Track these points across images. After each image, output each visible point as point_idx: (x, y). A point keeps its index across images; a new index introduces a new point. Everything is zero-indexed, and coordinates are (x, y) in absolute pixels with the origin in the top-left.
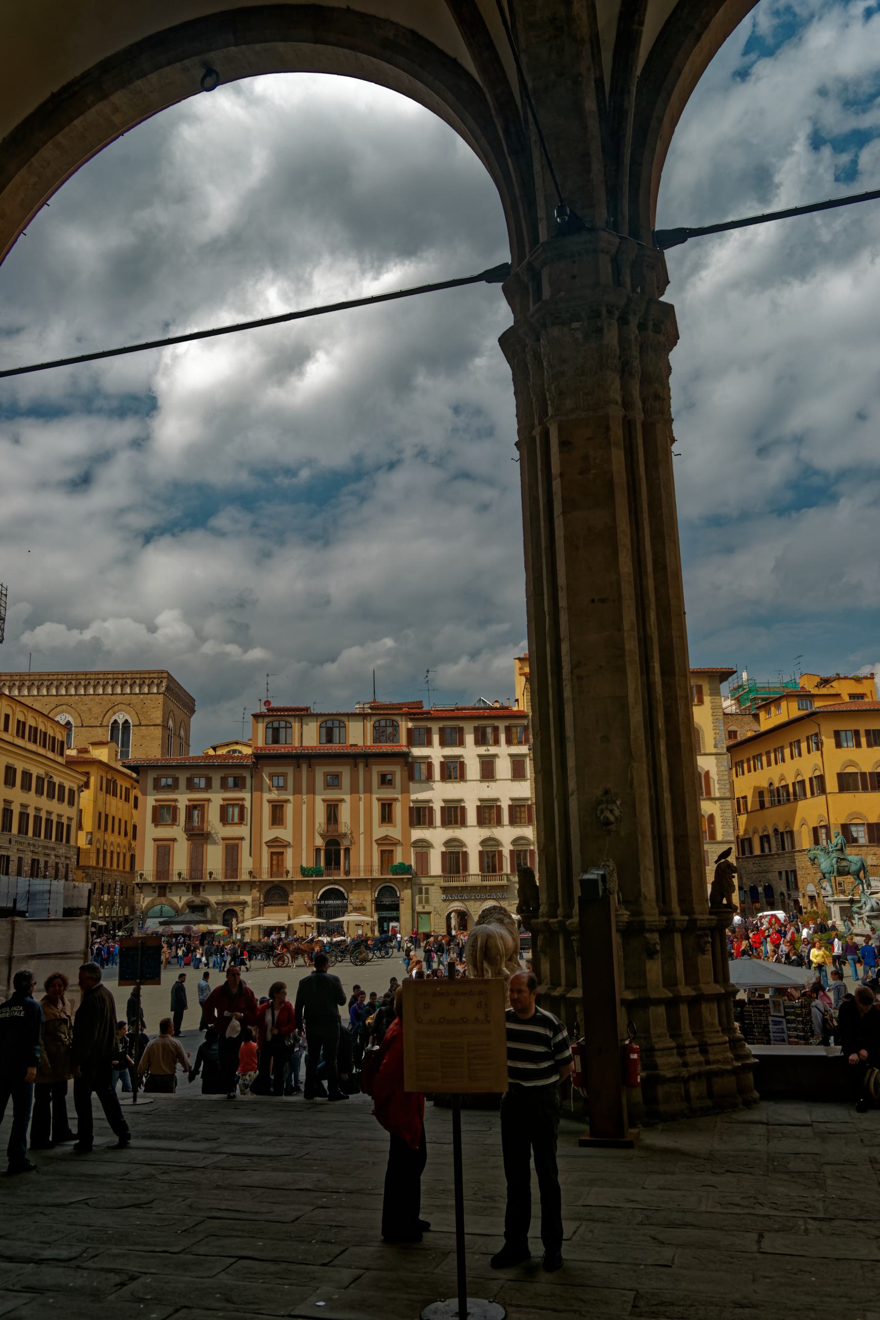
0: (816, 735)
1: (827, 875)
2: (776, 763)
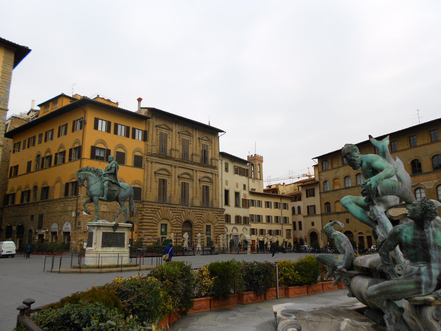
0: (82, 118)
1: (95, 198)
2: (46, 141)
